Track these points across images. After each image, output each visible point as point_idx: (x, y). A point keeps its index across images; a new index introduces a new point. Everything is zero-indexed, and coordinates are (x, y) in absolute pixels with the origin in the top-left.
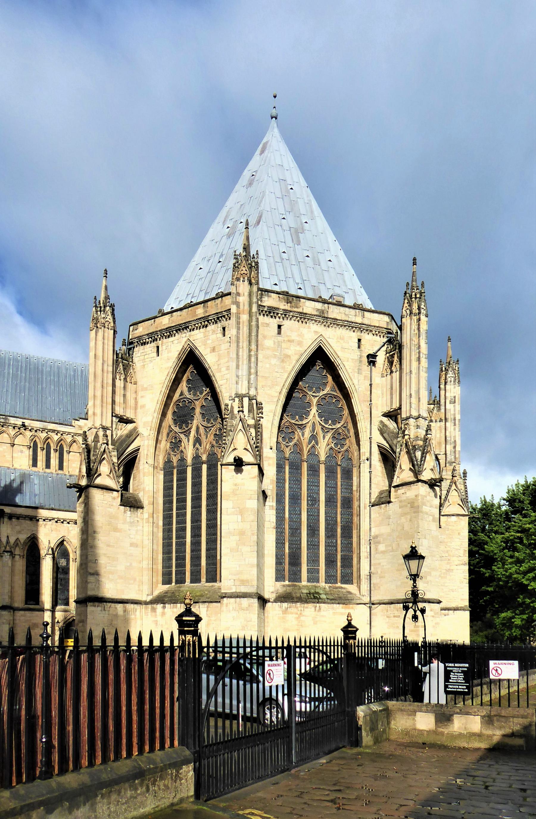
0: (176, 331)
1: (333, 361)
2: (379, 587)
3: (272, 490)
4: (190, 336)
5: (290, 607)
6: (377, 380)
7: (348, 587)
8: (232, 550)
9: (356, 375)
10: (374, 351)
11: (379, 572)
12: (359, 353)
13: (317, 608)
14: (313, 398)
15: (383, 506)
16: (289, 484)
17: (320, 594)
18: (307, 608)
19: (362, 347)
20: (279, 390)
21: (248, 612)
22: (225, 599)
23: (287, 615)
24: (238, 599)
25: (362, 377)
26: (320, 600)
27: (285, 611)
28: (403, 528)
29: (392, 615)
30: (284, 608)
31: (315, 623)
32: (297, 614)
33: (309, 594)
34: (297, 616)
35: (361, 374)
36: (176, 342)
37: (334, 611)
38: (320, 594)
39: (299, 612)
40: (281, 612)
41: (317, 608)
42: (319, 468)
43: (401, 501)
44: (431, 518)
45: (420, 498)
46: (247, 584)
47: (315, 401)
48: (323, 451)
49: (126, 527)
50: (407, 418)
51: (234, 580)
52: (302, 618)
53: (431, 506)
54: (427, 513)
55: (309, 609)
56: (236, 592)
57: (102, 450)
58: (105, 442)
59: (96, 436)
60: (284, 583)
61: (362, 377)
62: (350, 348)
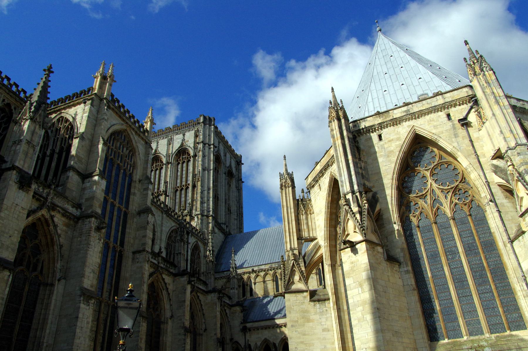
0: (324, 170)
1: (430, 138)
3: (404, 257)
8: (359, 320)
9: (454, 140)
14: (426, 172)
15: (520, 238)
19: (453, 118)
35: (458, 137)
36: (326, 177)
42: (450, 224)
47: (428, 174)
49: (317, 317)
51: (366, 349)
57: (291, 265)
59: (289, 256)
61: (460, 139)
62: (441, 123)
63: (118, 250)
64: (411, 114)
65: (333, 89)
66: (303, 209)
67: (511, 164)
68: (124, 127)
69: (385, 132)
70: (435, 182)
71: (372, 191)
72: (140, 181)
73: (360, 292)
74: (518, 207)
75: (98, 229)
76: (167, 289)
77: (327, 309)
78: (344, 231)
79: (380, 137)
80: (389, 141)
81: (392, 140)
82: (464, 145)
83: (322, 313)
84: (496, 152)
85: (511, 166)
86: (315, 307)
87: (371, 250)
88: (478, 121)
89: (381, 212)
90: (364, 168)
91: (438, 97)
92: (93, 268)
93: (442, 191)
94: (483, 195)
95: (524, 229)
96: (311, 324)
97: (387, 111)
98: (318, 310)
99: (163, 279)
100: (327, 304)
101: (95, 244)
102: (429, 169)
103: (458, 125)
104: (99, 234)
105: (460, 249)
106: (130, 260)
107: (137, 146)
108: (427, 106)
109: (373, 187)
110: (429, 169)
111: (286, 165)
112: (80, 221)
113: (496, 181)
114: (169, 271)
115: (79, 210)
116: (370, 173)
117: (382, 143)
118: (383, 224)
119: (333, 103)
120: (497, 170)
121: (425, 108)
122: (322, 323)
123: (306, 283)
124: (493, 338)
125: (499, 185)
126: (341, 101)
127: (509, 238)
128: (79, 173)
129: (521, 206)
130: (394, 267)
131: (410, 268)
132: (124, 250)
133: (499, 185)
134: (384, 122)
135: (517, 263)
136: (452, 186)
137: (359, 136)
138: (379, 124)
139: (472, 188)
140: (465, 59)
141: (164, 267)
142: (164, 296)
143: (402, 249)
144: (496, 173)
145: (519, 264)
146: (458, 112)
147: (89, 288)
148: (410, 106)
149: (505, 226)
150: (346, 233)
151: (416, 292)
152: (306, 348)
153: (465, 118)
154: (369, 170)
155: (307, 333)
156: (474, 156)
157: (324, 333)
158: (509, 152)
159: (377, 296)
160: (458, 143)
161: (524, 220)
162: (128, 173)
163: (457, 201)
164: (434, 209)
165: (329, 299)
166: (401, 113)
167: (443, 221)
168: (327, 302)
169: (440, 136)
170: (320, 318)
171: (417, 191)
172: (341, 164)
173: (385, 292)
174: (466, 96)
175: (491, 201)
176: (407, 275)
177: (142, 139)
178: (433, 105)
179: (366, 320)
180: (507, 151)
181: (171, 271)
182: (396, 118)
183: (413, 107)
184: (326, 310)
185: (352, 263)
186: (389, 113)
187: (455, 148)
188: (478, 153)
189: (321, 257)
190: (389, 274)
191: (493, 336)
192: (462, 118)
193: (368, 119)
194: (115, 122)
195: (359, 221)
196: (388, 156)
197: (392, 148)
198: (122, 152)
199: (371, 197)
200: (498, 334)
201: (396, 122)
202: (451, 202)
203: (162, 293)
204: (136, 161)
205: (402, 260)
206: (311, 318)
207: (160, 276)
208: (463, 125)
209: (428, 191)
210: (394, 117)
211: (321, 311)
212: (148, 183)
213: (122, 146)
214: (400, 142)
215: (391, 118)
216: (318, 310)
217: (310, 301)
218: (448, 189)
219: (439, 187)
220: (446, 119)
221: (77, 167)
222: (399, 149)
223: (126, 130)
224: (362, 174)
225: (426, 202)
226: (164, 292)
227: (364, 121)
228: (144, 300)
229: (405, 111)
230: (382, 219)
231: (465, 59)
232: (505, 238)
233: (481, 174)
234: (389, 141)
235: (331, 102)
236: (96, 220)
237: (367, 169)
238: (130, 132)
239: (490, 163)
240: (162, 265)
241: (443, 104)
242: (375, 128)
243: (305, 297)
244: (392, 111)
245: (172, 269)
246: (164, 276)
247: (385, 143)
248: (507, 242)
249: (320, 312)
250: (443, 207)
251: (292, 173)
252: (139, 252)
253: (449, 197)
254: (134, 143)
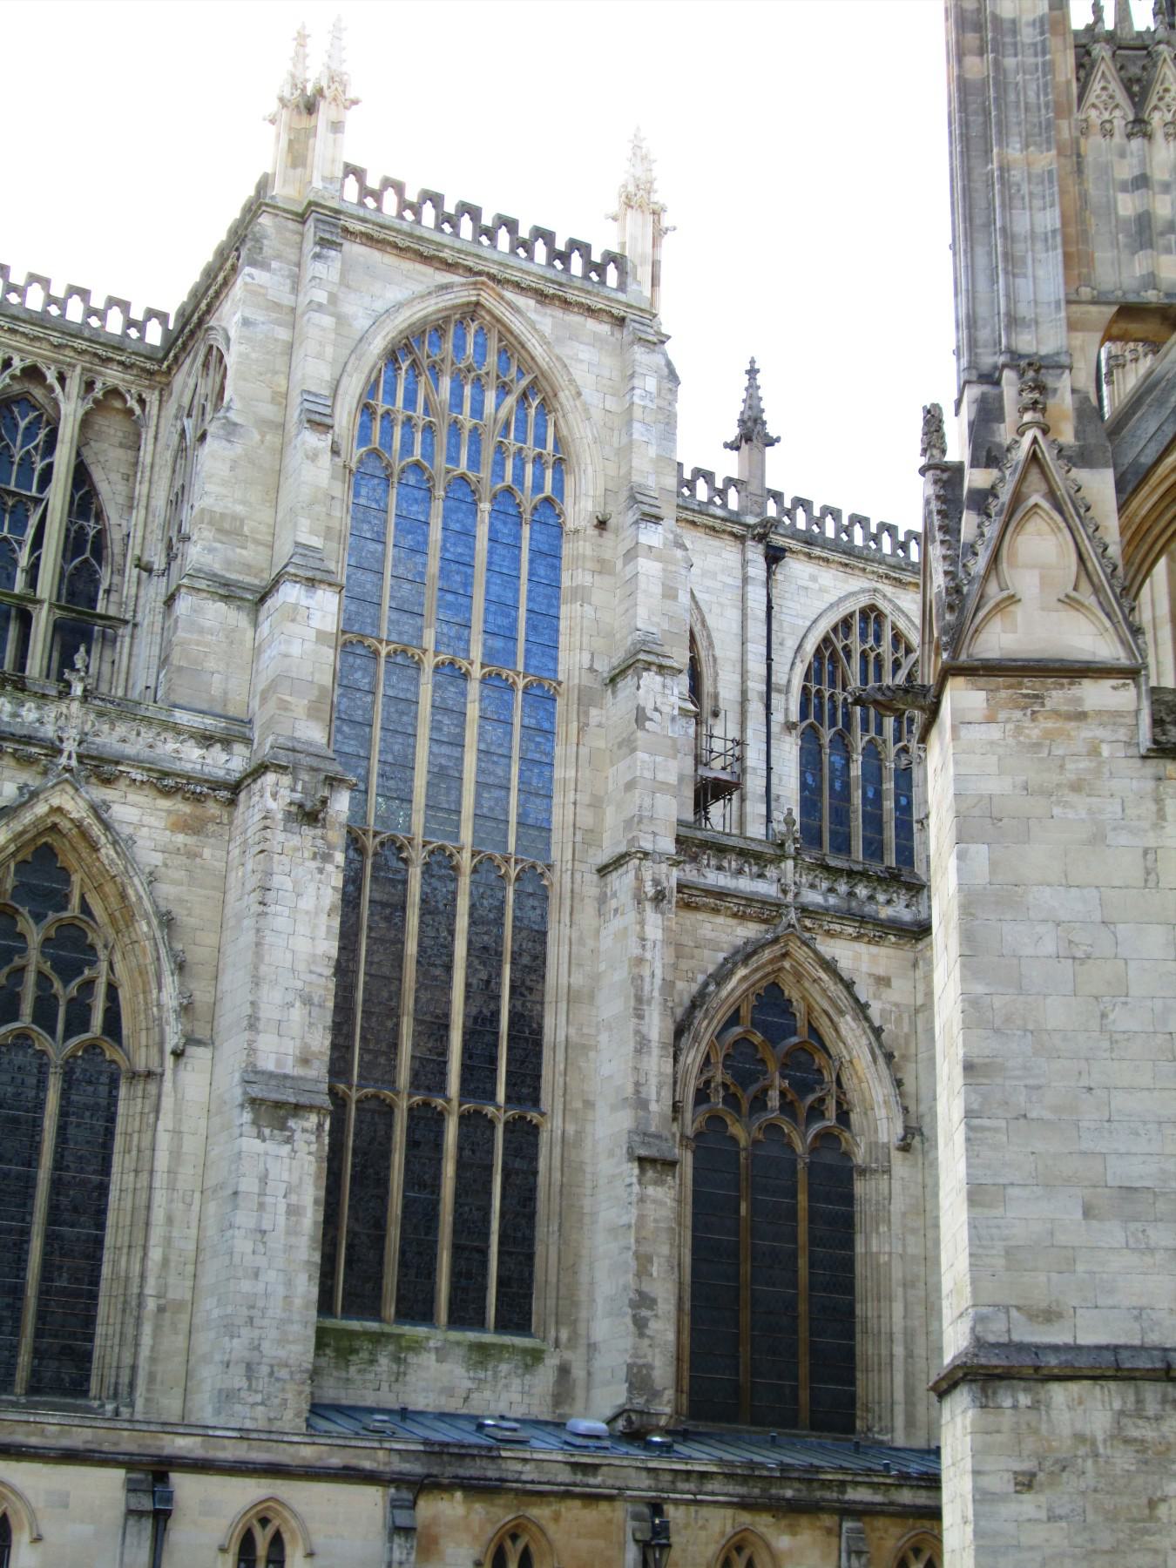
63: (513, 874)
68: (466, 296)
72: (602, 524)
75: (309, 815)
76: (862, 1009)
92: (299, 985)
99: (829, 966)
101: (295, 883)
104: (319, 832)
106: (590, 908)
107: (559, 358)
112: (243, 796)
114: (863, 920)
115: (238, 748)
128: (227, 591)
132: (549, 867)
141: (832, 900)
142: (850, 1041)
147: (290, 1068)
159: (979, 989)
162: (528, 499)
177: (590, 311)
181: (885, 913)
194: (394, 294)
198: (477, 411)
203: (837, 1030)
204: (569, 429)
207: (801, 953)
212: (636, 522)
213: (468, 390)
221: (217, 567)
223: (478, 304)
226: (849, 1025)
228: (653, 1081)
236: (286, 780)
238: (500, 310)
240: (813, 898)
245: (889, 902)
246: (831, 948)
252: (619, 861)
254: (538, 351)
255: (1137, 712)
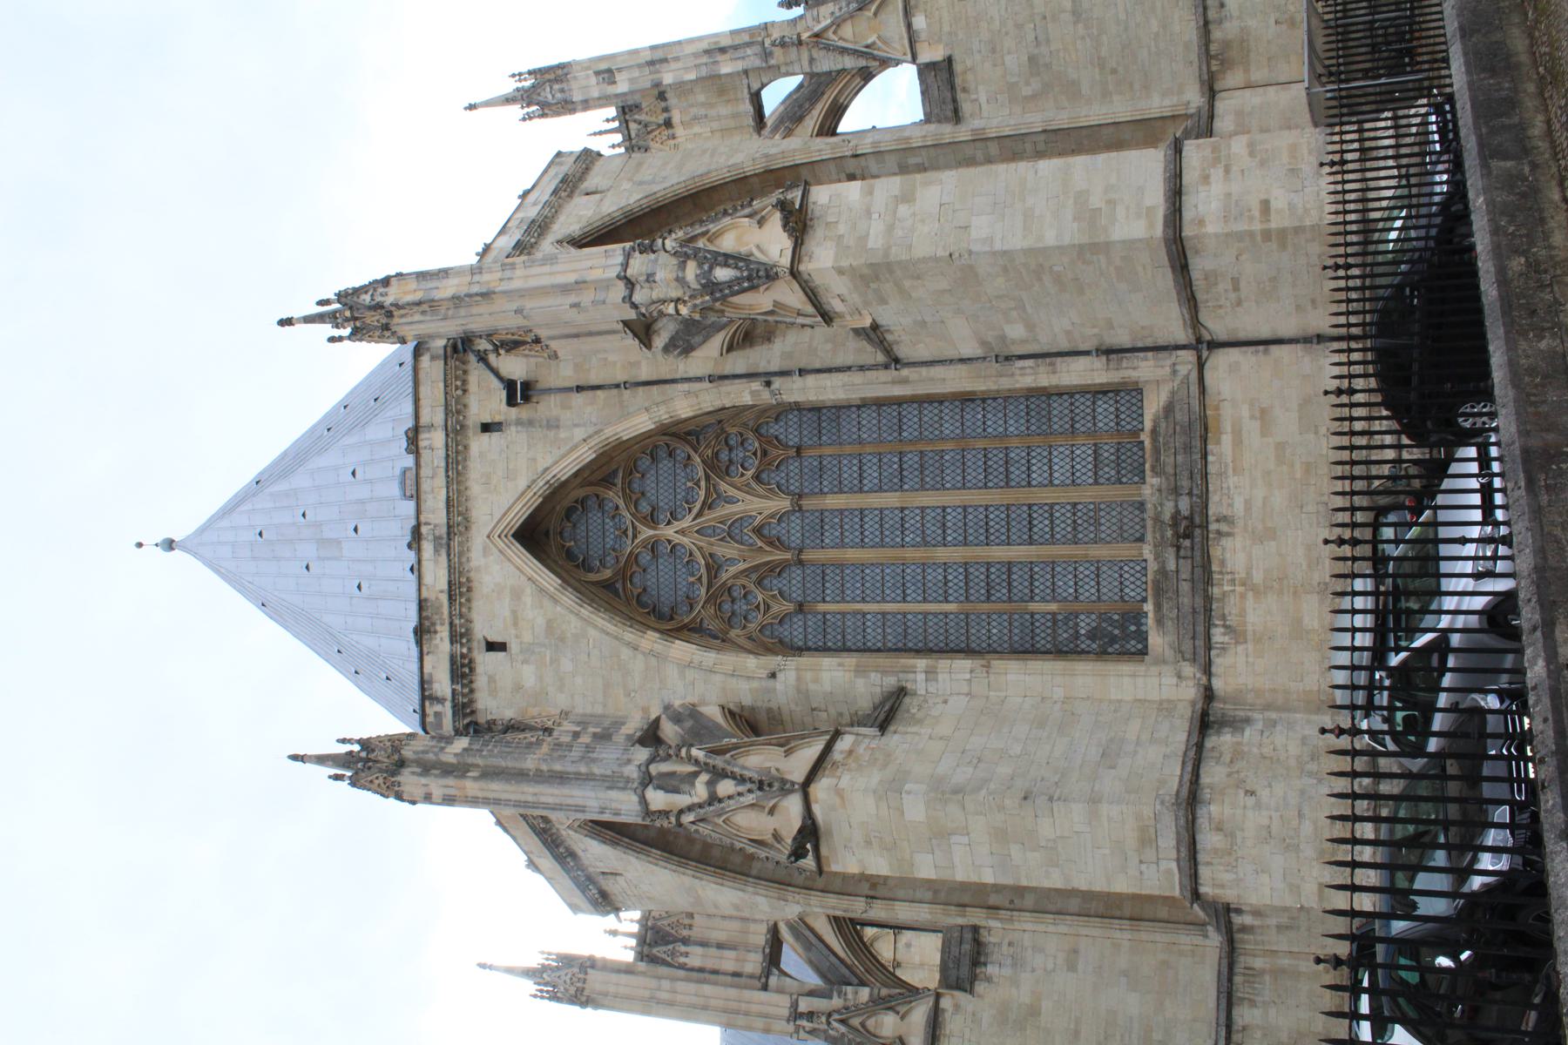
0: (557, 846)
2: (1143, 328)
3: (884, 673)
4: (562, 824)
5: (1224, 617)
6: (564, 374)
7: (1153, 406)
9: (563, 435)
10: (501, 386)
11: (1096, 331)
12: (513, 428)
13: (1224, 527)
14: (640, 538)
16: (863, 600)
17: (1178, 512)
18: (1223, 563)
19: (497, 419)
20: (626, 653)
21: (1239, 834)
22: (1202, 890)
23: (1250, 628)
24: (1201, 857)
25: (566, 416)
26: (1197, 520)
27: (1237, 634)
28: (944, 291)
29: (1233, 296)
30: (1226, 639)
31: (1270, 534)
32: (1243, 596)
33: (1178, 548)
34: (1250, 594)
35: (558, 420)
37: (1230, 471)
38: (1178, 512)
39: (1239, 589)
40: (1240, 648)
41: (1224, 527)
43: (867, 304)
44: (903, 210)
45: (845, 263)
46: (1152, 831)
47: (646, 533)
48: (770, 503)
50: (635, 306)
51: (1141, 862)
52: (1258, 577)
53: (868, 213)
54: (890, 228)
55: (1228, 555)
56: (1178, 860)
57: (843, 1029)
58: (824, 1019)
60: (1151, 615)
61: (566, 416)
64: (449, 534)
65: (295, 758)
66: (671, 947)
67: (672, 305)
69: (484, 626)
70: (676, 519)
71: (657, 720)
73: (965, 840)
74: (800, 320)
77: (1006, 941)
78: (760, 843)
79: (492, 646)
80: (515, 624)
81: (514, 613)
82: (589, 409)
83: (1017, 963)
84: (632, 331)
85: (680, 307)
86: (995, 980)
87: (838, 774)
88: (527, 352)
89: (732, 707)
90: (579, 724)
91: (422, 444)
93: (708, 505)
94: (747, 399)
95: (867, 323)
96: (1046, 1005)
97: (422, 604)
98: (1007, 972)
100: (992, 939)
102: (634, 528)
103: (522, 412)
105: (891, 499)
108: (441, 481)
109: (645, 710)
110: (634, 528)
111: (510, 971)
113: (716, 353)
116: (599, 710)
117: (514, 647)
118: (769, 710)
119: (339, 772)
120: (683, 344)
121: (444, 491)
122: (1050, 966)
123: (912, 992)
124: (1155, 481)
125: (730, 349)
126: (343, 741)
127: (886, 367)
129: (799, 314)
130: (908, 711)
131: (921, 663)
133: (730, 349)
134: (451, 624)
135: (960, 366)
136: (701, 473)
137: (473, 712)
138: (454, 638)
139: (720, 422)
140: (332, 340)
143: (860, 671)
144: (688, 350)
145: (962, 360)
146: (486, 400)
148: (424, 530)
149: (849, 368)
150: (768, 838)
151: (998, 664)
152: (1118, 1038)
153: (510, 385)
154: (589, 710)
155: (1072, 1026)
156: (628, 391)
157: (1080, 967)
158: (637, 298)
160: (576, 425)
161: (841, 316)
163: (750, 473)
164: (760, 544)
165: (975, 929)
166: (436, 562)
167: (798, 528)
168: (985, 937)
169: (540, 469)
170: (1033, 970)
171: (691, 579)
172: (543, 799)
173: (980, 760)
174: (446, 364)
175: (768, 384)
176: (940, 677)
178: (443, 464)
179: (1054, 841)
180: (635, 306)
182: (450, 582)
183: (428, 524)
184: (1010, 944)
185: (868, 843)
186: (426, 600)
187: (590, 437)
188: (620, 377)
189: (837, 922)
190: (925, 731)
191: (1153, 480)
192: (504, 394)
193: (427, 670)
195: (741, 789)
196: (562, 639)
197: (540, 621)
199: (676, 728)
200: (1147, 466)
201: (459, 588)
202: (749, 491)
205: (891, 682)
206: (1028, 1001)
208: (526, 398)
209: (700, 549)
210: (446, 587)
211: (1009, 961)
214: (528, 591)
215: (444, 598)
216: (1007, 972)
217: (972, 992)
218: (707, 489)
219: (695, 511)
220: (495, 435)
222: (547, 602)
224: (595, 735)
225: (731, 561)
227: (431, 682)
229: (436, 551)
230: (753, 709)
231: (332, 340)
232: (884, 375)
233: (686, 386)
234: (515, 624)
235: (337, 777)
237: (585, 715)
239: (660, 356)
241: (447, 435)
242: (463, 656)
243: (957, 1007)
244: (424, 589)
247: (517, 637)
248: (895, 373)
249: (1014, 965)
250: (759, 518)
251: (543, 953)
253: (732, 492)
255: (857, 734)
